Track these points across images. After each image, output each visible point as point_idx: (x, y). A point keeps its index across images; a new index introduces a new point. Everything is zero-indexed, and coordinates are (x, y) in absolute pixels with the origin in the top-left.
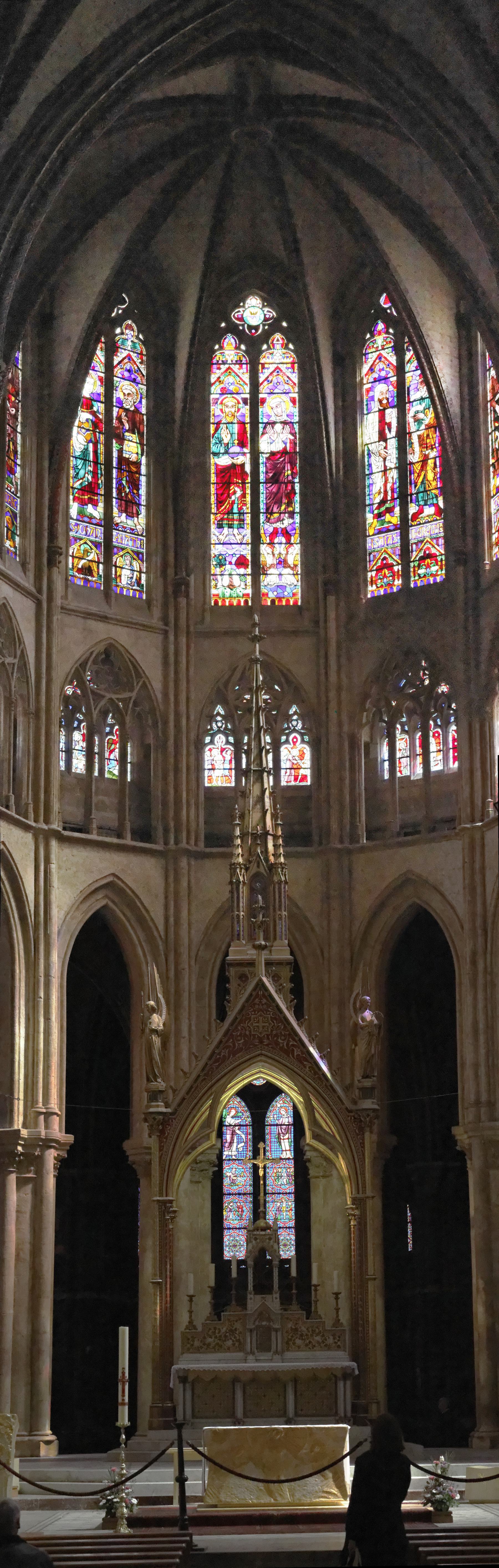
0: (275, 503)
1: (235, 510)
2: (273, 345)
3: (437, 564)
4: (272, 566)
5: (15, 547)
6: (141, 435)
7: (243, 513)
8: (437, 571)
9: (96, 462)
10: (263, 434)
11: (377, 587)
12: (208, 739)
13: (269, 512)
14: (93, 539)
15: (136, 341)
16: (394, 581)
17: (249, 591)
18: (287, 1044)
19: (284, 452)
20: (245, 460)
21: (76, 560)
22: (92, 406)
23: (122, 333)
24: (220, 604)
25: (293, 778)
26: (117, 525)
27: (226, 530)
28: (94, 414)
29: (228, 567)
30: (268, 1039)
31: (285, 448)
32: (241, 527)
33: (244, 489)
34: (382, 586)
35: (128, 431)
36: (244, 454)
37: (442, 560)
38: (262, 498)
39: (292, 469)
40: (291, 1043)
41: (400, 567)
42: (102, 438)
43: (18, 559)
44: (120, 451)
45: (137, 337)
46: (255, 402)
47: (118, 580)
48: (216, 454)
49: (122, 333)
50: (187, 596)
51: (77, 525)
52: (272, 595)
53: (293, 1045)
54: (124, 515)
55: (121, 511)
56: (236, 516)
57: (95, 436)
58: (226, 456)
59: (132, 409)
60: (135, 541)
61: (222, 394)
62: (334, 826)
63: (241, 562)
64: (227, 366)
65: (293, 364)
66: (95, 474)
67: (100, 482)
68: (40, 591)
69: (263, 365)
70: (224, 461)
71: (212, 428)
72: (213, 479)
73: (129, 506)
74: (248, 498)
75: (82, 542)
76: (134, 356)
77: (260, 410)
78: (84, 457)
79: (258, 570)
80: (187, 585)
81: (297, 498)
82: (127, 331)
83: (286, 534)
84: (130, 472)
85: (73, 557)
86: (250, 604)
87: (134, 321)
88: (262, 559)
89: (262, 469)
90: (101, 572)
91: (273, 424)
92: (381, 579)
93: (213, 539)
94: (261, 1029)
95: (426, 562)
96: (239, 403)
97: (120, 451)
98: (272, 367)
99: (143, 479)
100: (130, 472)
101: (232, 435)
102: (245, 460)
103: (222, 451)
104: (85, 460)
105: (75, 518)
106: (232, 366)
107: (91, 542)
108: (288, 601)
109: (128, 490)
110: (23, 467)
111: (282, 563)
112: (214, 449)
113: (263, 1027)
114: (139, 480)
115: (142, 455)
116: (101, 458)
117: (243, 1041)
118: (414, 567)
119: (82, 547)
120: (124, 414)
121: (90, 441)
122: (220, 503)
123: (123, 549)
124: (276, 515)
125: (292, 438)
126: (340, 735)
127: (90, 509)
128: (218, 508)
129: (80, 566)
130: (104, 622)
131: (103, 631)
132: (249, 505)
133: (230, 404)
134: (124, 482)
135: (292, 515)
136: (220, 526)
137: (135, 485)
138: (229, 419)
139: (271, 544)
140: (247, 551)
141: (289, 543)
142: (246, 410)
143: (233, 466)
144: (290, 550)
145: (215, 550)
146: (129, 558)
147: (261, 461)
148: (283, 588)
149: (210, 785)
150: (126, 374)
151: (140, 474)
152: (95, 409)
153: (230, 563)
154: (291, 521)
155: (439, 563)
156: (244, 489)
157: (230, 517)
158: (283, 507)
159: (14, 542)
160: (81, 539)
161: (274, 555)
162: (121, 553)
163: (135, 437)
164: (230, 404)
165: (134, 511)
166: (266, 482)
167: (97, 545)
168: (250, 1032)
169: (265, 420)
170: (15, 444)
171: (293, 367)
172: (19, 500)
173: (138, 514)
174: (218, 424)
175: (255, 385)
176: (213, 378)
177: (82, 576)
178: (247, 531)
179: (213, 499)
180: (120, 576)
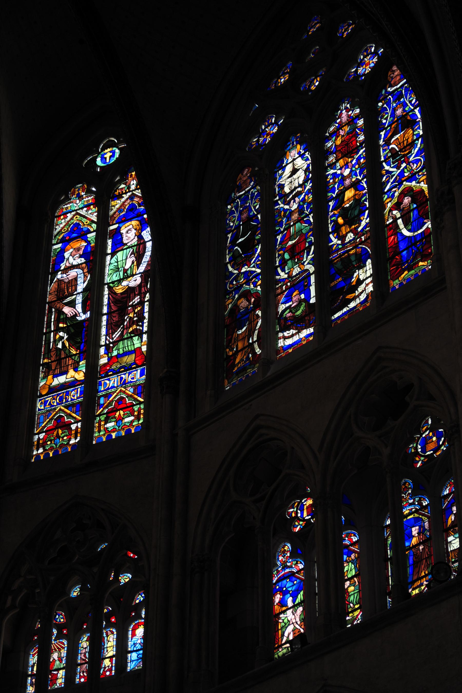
3: (133, 415)
8: (132, 422)
11: (45, 450)
16: (70, 440)
34: (52, 448)
37: (139, 409)
41: (79, 425)
92: (51, 441)
95: (118, 414)
118: (100, 421)
155: (136, 413)
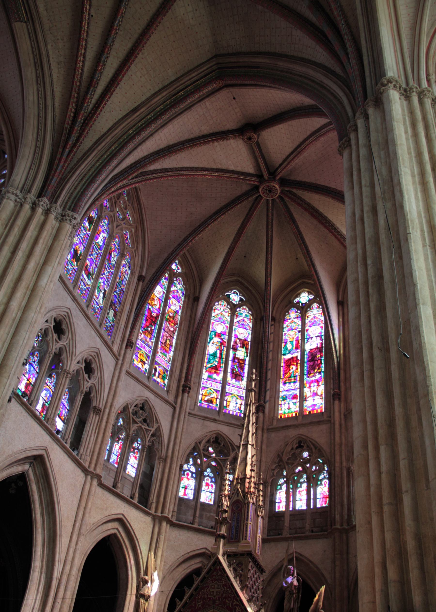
0: (312, 369)
1: (292, 375)
2: (313, 309)
4: (309, 397)
5: (164, 383)
6: (247, 349)
7: (296, 376)
9: (221, 358)
10: (307, 342)
12: (279, 487)
13: (309, 373)
14: (215, 388)
15: (248, 314)
17: (298, 409)
18: (232, 604)
19: (317, 347)
20: (298, 354)
21: (204, 397)
22: (221, 336)
23: (240, 311)
24: (283, 417)
25: (324, 503)
26: (230, 384)
27: (287, 384)
28: (222, 339)
29: (288, 400)
30: (219, 600)
31: (317, 347)
32: (295, 382)
33: (297, 366)
35: (240, 347)
36: (298, 352)
38: (305, 368)
39: (320, 354)
40: (235, 603)
42: (225, 349)
43: (165, 389)
44: (235, 355)
45: (248, 313)
46: (303, 331)
47: (228, 407)
48: (284, 355)
49: (240, 311)
50: (264, 412)
51: (206, 382)
52: (309, 409)
53: (236, 605)
54: (234, 380)
55: (232, 378)
56: (292, 378)
57: (221, 348)
58: (290, 354)
59: (243, 339)
60: (239, 392)
61: (288, 331)
62: (338, 517)
63: (295, 397)
64: (291, 320)
65: (321, 313)
66: (219, 362)
67: (222, 365)
68: (176, 404)
69: (308, 317)
70: (288, 356)
71: (283, 345)
72: (282, 364)
73: (237, 376)
74: (299, 370)
75: (208, 389)
76: (246, 319)
77: (306, 333)
78: (214, 355)
79: (303, 399)
80: (264, 407)
81: (323, 365)
82: (243, 310)
83: (317, 381)
84: (239, 363)
85: (202, 395)
86: (298, 415)
87: (247, 307)
88: (304, 394)
89: (306, 356)
90: (218, 403)
91: (312, 338)
93: (281, 389)
94: (215, 594)
96: (296, 333)
97: (235, 355)
98: (312, 317)
99: (246, 367)
100: (239, 363)
101: (292, 345)
102: (298, 354)
103: (287, 352)
104: (215, 356)
105: (206, 379)
106: (294, 320)
107: (214, 390)
108: (317, 411)
109: (237, 370)
110: (174, 352)
111: (315, 394)
112: (283, 352)
113: (217, 591)
114: (244, 366)
115: (247, 356)
116: (224, 356)
117: (202, 602)
119: (208, 392)
120: (238, 341)
121: (219, 349)
122: (285, 374)
123: (232, 394)
124: (312, 375)
125: (321, 342)
126: (341, 469)
127: (215, 376)
128: (284, 376)
129: (206, 399)
130: (215, 422)
131: (213, 427)
132: (299, 373)
133: (292, 334)
134: (235, 367)
135: (320, 373)
136: (285, 384)
137: (242, 368)
138: (291, 340)
139: (310, 387)
140: (297, 392)
141: (318, 385)
142: (299, 335)
143: (293, 358)
144: (319, 388)
145: (281, 394)
146: (235, 398)
147: (306, 353)
148: (315, 405)
149: (278, 510)
150: (241, 326)
151: (245, 364)
152: (222, 337)
153: (289, 398)
154: (320, 376)
156: (297, 366)
157: (290, 379)
158: (316, 371)
159: (164, 381)
160: (208, 388)
161: (311, 391)
162: (231, 396)
163: (244, 350)
164: (292, 334)
165: (240, 379)
166: (307, 362)
167: (217, 391)
168: (208, 595)
169: (308, 337)
170: (171, 342)
171: (322, 315)
172: (170, 365)
173: (242, 380)
174: (286, 343)
175: (304, 324)
176: (285, 326)
177: (206, 403)
178: (298, 384)
179: (282, 373)
180: (229, 405)
